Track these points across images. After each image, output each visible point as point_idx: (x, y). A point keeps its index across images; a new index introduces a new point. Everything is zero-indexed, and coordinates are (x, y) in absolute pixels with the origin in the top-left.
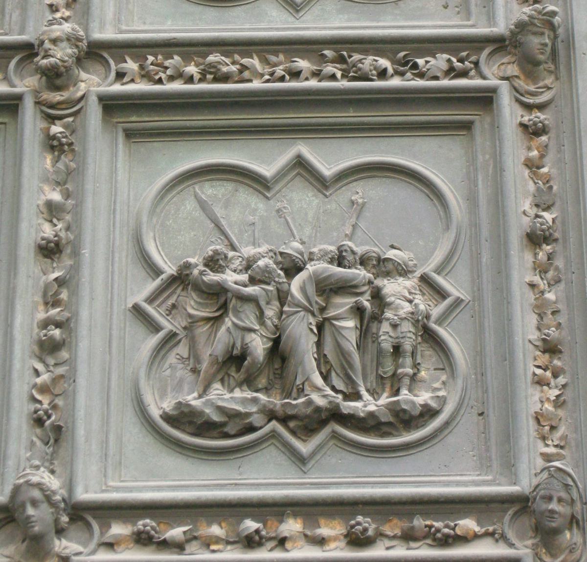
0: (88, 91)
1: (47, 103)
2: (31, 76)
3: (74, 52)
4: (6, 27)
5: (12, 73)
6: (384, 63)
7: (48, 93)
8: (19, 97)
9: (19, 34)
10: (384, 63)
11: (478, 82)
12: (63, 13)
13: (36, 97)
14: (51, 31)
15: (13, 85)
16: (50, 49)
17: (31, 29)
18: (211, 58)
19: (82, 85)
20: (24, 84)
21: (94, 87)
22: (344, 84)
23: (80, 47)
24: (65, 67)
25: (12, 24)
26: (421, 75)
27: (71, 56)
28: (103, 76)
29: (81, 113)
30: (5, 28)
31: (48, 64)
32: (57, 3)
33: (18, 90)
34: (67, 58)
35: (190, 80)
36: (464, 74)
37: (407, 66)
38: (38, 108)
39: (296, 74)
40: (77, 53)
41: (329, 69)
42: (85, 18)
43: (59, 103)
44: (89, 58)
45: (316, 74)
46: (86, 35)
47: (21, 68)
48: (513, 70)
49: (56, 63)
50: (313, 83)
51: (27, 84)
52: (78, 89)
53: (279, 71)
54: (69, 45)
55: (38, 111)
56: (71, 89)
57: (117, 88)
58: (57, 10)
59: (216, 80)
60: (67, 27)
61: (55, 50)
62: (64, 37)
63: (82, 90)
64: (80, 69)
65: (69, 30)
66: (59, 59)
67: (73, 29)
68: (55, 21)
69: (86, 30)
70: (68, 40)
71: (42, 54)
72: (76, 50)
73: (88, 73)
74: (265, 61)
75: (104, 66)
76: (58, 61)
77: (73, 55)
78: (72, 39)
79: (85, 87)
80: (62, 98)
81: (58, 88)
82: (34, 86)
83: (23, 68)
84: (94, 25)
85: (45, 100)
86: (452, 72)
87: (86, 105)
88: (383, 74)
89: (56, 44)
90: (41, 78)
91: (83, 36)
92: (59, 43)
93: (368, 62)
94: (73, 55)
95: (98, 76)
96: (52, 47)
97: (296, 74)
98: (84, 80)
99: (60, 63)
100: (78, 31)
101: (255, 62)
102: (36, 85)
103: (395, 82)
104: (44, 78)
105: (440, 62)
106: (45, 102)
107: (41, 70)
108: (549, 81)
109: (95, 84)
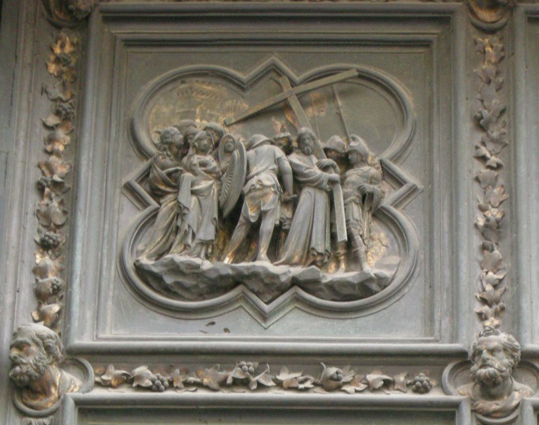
0: (523, 401)
1: (483, 411)
2: (465, 383)
3: (511, 363)
4: (437, 333)
5: (447, 381)
7: (484, 401)
8: (456, 405)
9: (451, 342)
12: (492, 322)
13: (472, 405)
14: (489, 341)
15: (446, 392)
16: (488, 359)
19: (516, 395)
20: (458, 391)
21: (528, 396)
23: (516, 357)
24: (502, 377)
25: (442, 331)
27: (507, 366)
29: (517, 423)
30: (435, 335)
31: (487, 374)
32: (487, 312)
33: (455, 398)
34: (504, 368)
38: (474, 416)
40: (514, 363)
42: (516, 327)
43: (495, 412)
44: (521, 367)
47: (454, 376)
49: (494, 372)
51: (461, 392)
52: (513, 399)
54: (506, 356)
55: (475, 419)
56: (506, 397)
58: (486, 319)
60: (503, 337)
61: (492, 360)
62: (501, 347)
63: (516, 400)
64: (513, 378)
65: (506, 340)
66: (496, 369)
67: (509, 340)
68: (492, 331)
69: (518, 339)
70: (505, 350)
71: (480, 363)
72: (512, 361)
73: (520, 381)
75: (535, 375)
76: (495, 370)
77: (510, 364)
78: (508, 349)
79: (519, 396)
80: (497, 407)
81: (493, 397)
82: (468, 394)
83: (456, 376)
84: (526, 335)
85: (480, 409)
87: (521, 414)
89: (494, 353)
91: (518, 347)
92: (496, 353)
94: (510, 364)
95: (530, 385)
96: (490, 357)
98: (518, 388)
99: (498, 374)
100: (513, 342)
102: (470, 392)
104: (478, 386)
106: (481, 411)
107: (479, 380)
109: (529, 394)
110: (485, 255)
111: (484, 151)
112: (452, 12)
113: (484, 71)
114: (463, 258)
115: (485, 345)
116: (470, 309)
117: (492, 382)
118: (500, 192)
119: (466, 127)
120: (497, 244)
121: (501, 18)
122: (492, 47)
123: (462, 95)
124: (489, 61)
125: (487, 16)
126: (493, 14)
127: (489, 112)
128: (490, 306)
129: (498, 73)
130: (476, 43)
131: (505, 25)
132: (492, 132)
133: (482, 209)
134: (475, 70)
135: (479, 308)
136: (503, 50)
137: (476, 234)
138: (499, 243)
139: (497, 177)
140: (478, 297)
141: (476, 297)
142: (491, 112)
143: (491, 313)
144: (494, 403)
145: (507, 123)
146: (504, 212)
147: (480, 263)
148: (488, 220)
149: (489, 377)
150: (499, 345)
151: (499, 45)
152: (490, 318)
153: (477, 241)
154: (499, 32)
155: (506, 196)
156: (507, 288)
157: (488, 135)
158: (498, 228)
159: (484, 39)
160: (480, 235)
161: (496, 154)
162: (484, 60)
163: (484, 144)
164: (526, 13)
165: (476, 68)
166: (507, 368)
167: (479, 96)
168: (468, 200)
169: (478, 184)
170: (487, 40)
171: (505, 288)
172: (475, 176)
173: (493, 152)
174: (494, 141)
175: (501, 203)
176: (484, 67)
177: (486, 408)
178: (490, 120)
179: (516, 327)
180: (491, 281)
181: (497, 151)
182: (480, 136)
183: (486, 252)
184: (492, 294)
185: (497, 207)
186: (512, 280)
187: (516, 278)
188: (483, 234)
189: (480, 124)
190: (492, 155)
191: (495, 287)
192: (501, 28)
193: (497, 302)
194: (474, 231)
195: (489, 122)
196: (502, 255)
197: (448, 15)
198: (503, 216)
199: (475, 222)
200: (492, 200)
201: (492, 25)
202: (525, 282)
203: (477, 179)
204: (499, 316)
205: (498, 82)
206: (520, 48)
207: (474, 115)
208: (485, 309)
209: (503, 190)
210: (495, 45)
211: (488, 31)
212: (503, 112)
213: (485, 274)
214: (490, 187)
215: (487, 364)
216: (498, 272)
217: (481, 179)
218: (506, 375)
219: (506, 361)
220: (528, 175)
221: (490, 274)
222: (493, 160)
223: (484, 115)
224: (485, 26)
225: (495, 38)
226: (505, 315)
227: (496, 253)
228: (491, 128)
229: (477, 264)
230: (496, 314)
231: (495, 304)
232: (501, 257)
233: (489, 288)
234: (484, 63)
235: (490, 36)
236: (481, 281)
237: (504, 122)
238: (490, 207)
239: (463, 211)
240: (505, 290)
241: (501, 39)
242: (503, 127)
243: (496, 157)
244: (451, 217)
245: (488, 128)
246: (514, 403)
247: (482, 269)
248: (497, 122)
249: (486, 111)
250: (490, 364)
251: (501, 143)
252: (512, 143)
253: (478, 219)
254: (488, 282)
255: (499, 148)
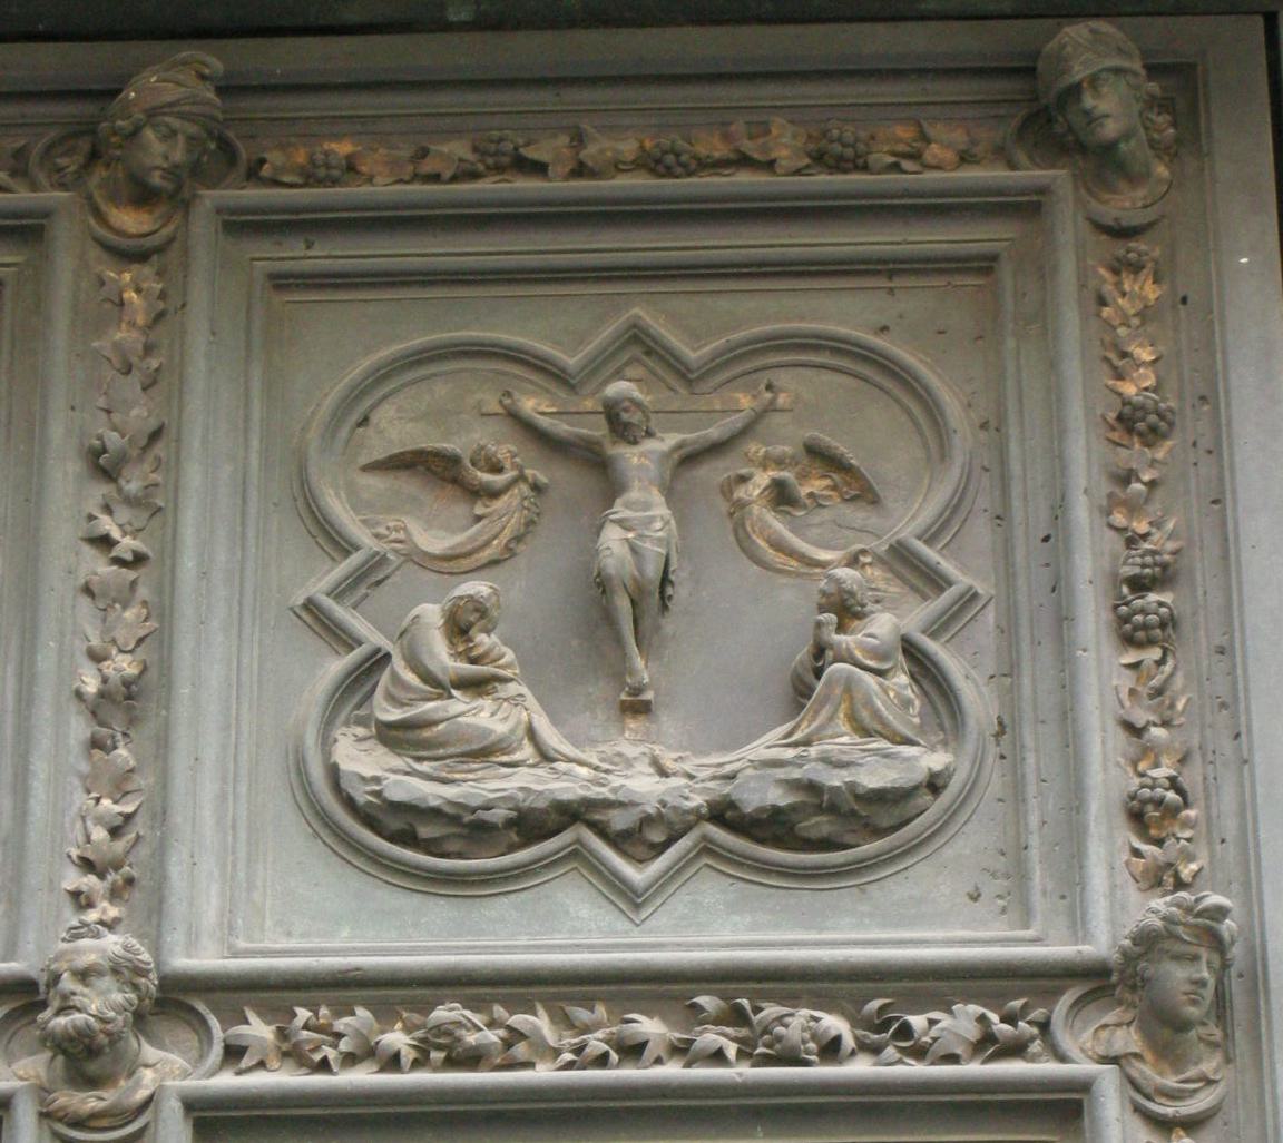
0: (161, 1087)
1: (66, 1116)
2: (32, 1054)
6: (834, 1024)
10: (834, 1024)
11: (1047, 1068)
12: (104, 911)
13: (42, 1102)
14: (78, 952)
16: (74, 994)
17: (31, 947)
18: (441, 1014)
19: (148, 1076)
21: (174, 1079)
22: (744, 1072)
24: (109, 1034)
26: (919, 1053)
27: (120, 1009)
28: (195, 1053)
31: (69, 1027)
32: (91, 888)
34: (111, 1014)
35: (393, 1062)
36: (1016, 1049)
37: (886, 1031)
38: (45, 1127)
39: (633, 1050)
40: (136, 1002)
41: (710, 1038)
42: (154, 922)
43: (95, 1115)
44: (163, 1013)
45: (680, 1050)
46: (155, 961)
48: (1127, 1040)
49: (88, 1026)
50: (673, 1071)
51: (21, 1073)
52: (138, 1085)
53: (596, 1043)
54: (117, 984)
56: (122, 1083)
57: (227, 1081)
58: (90, 905)
59: (452, 1063)
60: (112, 943)
61: (84, 995)
62: (106, 965)
63: (147, 1087)
64: (140, 1037)
65: (118, 950)
67: (126, 948)
68: (85, 929)
69: (156, 949)
70: (115, 971)
71: (56, 1003)
72: (132, 996)
73: (160, 1046)
74: (564, 1021)
76: (92, 1019)
79: (154, 1080)
80: (102, 1105)
81: (93, 1083)
82: (38, 1077)
83: (12, 1037)
84: (175, 938)
85: (62, 1109)
86: (989, 1044)
87: (156, 1119)
88: (831, 1049)
89: (87, 981)
90: (53, 1058)
91: (149, 964)
93: (799, 1022)
94: (128, 1006)
95: (183, 1053)
96: (79, 988)
97: (633, 1050)
98: (151, 1062)
99: (96, 1025)
101: (540, 1023)
102: (43, 1073)
103: (860, 1068)
104: (60, 1058)
105: (961, 1022)
106: (61, 1114)
107: (53, 1041)
108: (1209, 1066)
109: (177, 1072)
110: (95, 758)
111: (107, 525)
112: (47, 214)
113: (117, 346)
114: (40, 767)
115: (67, 961)
116: (52, 884)
117: (82, 1046)
118: (138, 616)
119: (64, 475)
120: (125, 734)
121: (163, 226)
122: (138, 291)
123: (58, 403)
124: (132, 324)
125: (130, 221)
126: (145, 217)
127: (123, 437)
128: (102, 876)
129: (148, 350)
130: (103, 283)
131: (171, 240)
132: (128, 482)
133: (97, 657)
134: (96, 344)
135: (74, 879)
136: (163, 296)
137: (78, 713)
138: (132, 733)
139: (134, 584)
140: (74, 857)
141: (69, 857)
142: (126, 438)
143: (102, 892)
144: (91, 1097)
145: (164, 460)
146: (144, 662)
147: (83, 778)
148: (105, 680)
149: (73, 1034)
150: (101, 961)
151: (154, 285)
152: (98, 903)
153: (79, 728)
154: (155, 257)
155: (152, 624)
156: (141, 833)
157: (120, 490)
158: (129, 697)
159: (120, 273)
160: (90, 715)
161: (135, 533)
162: (120, 320)
163: (108, 510)
164: (219, 211)
165: (99, 338)
166: (117, 1013)
167: (102, 402)
168: (62, 634)
169: (89, 599)
170: (127, 277)
171: (137, 834)
172: (82, 581)
173: (128, 528)
174: (131, 502)
175: (140, 641)
176: (118, 336)
177: (72, 1109)
178: (124, 456)
179: (154, 922)
180: (107, 820)
181: (137, 525)
182: (101, 490)
183: (97, 753)
184: (105, 848)
185: (130, 652)
186: (154, 817)
187: (161, 815)
188: (94, 713)
189: (103, 466)
190: (125, 534)
191: (115, 832)
192: (160, 250)
193: (117, 867)
194: (74, 706)
195: (122, 459)
196: (137, 760)
197: (40, 221)
198: (144, 670)
199: (77, 684)
200: (120, 634)
201: (142, 241)
202: (179, 818)
203: (88, 590)
204: (120, 897)
205: (148, 368)
206: (199, 295)
207: (87, 445)
208: (90, 882)
209: (144, 611)
210: (145, 286)
211: (131, 255)
212: (156, 435)
213: (92, 802)
214: (117, 606)
215: (72, 1004)
216: (124, 800)
217: (96, 590)
218: (115, 1029)
219: (118, 997)
220: (204, 575)
221: (106, 802)
222: (127, 545)
223: (108, 444)
224: (123, 243)
225: (147, 270)
226: (137, 895)
227: (121, 755)
228: (125, 472)
229: (76, 782)
230: (115, 895)
231: (111, 871)
232: (132, 763)
233: (99, 834)
234: (119, 328)
235: (136, 267)
236: (83, 819)
237: (158, 460)
238: (114, 652)
239: (46, 661)
240: (138, 838)
241: (160, 274)
242: (153, 472)
243: (134, 539)
244: (20, 677)
245: (119, 474)
246: (141, 1095)
247: (89, 792)
248: (141, 458)
249: (115, 435)
250: (79, 1006)
251: (148, 506)
252: (171, 505)
253: (84, 678)
254: (99, 820)
255: (139, 519)
